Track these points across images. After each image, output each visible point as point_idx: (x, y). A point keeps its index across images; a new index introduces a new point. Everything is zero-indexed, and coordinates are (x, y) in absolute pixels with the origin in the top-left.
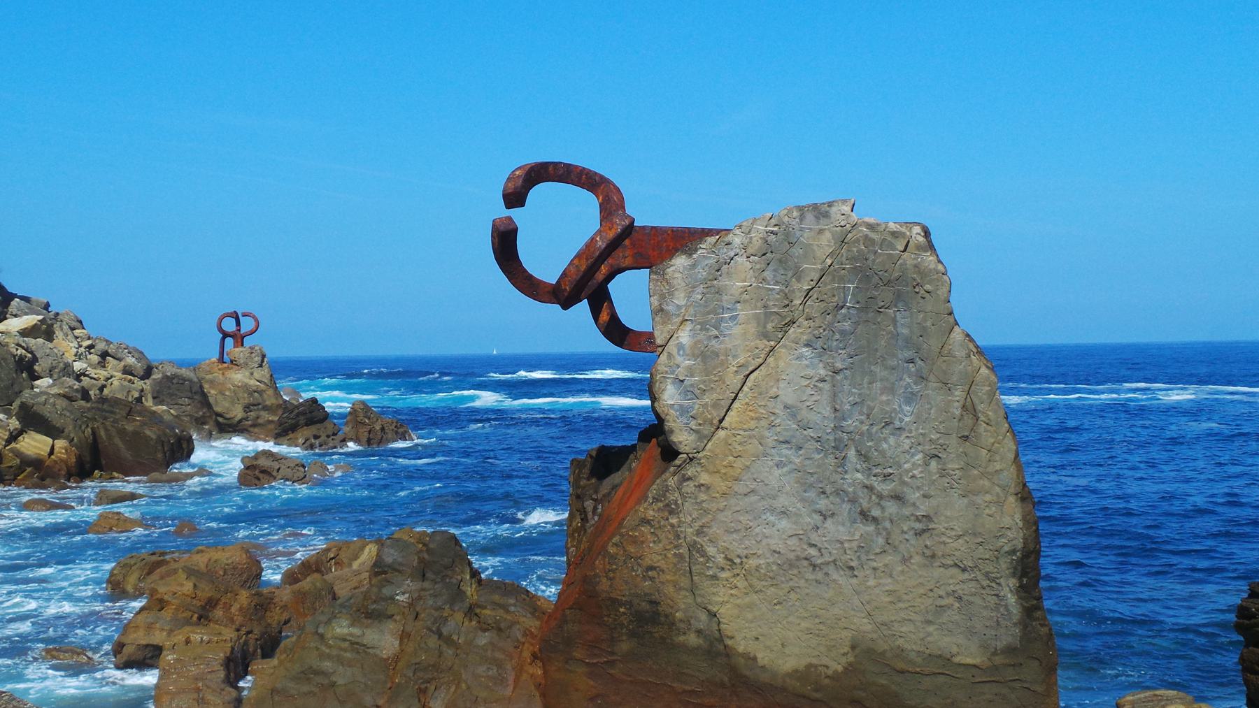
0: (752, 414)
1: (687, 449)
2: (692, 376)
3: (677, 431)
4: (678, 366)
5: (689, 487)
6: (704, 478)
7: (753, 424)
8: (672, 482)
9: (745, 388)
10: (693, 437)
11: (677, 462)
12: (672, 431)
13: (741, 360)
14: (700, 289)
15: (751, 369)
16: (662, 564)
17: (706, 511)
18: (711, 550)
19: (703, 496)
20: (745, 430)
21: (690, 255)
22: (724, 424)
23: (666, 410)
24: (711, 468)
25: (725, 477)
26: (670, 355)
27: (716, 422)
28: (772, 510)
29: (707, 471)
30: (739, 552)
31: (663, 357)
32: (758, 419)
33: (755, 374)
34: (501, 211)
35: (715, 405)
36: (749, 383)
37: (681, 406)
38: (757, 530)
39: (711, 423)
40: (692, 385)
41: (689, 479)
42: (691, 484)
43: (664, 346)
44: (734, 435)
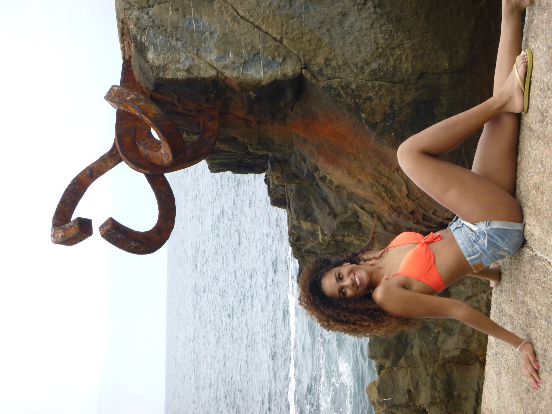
0: (270, 19)
1: (298, 67)
2: (241, 53)
3: (284, 72)
4: (234, 62)
5: (328, 72)
6: (320, 60)
7: (278, 18)
8: (323, 83)
9: (251, 19)
10: (288, 61)
11: (308, 76)
12: (285, 75)
13: (229, 19)
14: (174, 43)
15: (236, 14)
16: (388, 99)
17: (345, 63)
18: (374, 66)
19: (334, 63)
20: (283, 25)
21: (145, 47)
22: (278, 37)
23: (268, 77)
24: (312, 54)
25: (319, 47)
26: (225, 67)
27: (276, 44)
28: (341, 23)
29: (315, 56)
30: (374, 47)
31: (228, 73)
32: (274, 15)
33: (240, 12)
34: (96, 238)
35: (264, 42)
36: (247, 16)
37: (265, 66)
38: (357, 34)
39: (278, 47)
40: (249, 55)
41: (321, 70)
42: (325, 70)
43: (218, 72)
44: (287, 33)
